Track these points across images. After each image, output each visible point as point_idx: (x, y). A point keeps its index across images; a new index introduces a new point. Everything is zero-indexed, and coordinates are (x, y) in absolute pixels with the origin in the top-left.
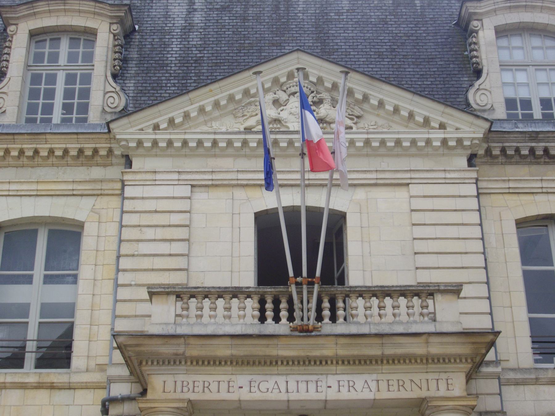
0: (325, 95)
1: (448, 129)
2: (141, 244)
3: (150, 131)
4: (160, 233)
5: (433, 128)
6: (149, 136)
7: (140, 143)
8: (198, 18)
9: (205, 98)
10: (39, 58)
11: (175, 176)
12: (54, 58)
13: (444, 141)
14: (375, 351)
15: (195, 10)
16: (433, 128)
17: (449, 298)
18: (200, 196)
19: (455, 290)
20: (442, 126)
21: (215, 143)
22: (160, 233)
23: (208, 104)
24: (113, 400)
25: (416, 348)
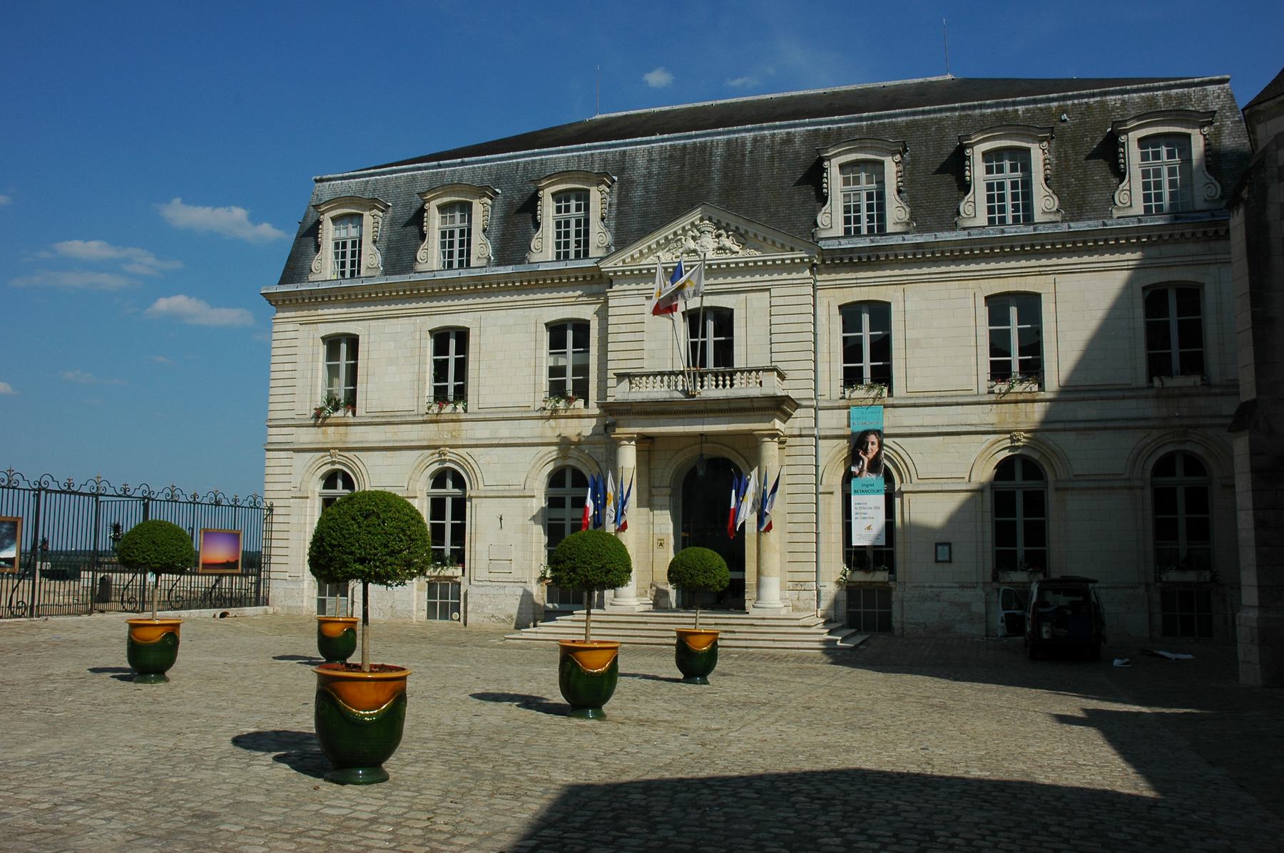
4: (629, 327)
8: (655, 169)
9: (651, 241)
10: (559, 210)
12: (567, 209)
22: (629, 327)
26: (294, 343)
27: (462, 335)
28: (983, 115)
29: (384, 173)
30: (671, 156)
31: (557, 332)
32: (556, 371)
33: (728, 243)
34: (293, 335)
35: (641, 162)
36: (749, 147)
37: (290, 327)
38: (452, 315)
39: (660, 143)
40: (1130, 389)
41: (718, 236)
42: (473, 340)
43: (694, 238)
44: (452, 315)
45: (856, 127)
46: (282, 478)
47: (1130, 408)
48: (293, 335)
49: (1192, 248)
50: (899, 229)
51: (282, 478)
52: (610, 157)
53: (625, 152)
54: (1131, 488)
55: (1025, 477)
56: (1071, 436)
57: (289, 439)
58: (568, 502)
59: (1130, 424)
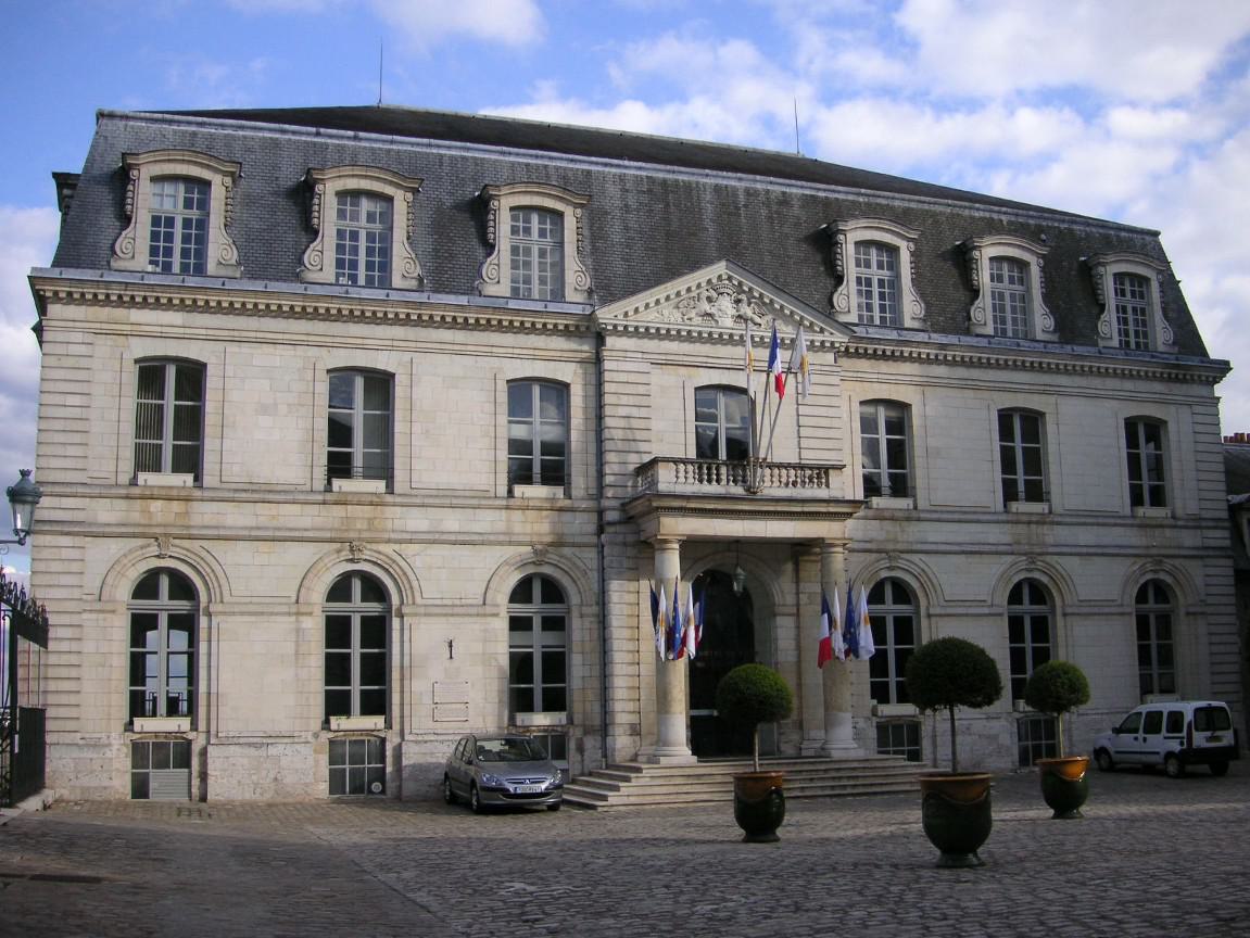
0: (743, 297)
1: (826, 333)
2: (620, 409)
3: (621, 317)
5: (816, 332)
6: (621, 322)
7: (615, 326)
9: (660, 292)
11: (640, 355)
13: (823, 342)
14: (799, 509)
15: (627, 191)
16: (816, 332)
17: (837, 472)
18: (656, 371)
19: (841, 468)
20: (822, 331)
21: (668, 330)
23: (662, 297)
24: (610, 524)
25: (822, 509)
26: (84, 363)
27: (381, 385)
28: (972, 218)
29: (189, 123)
30: (650, 191)
31: (519, 391)
32: (517, 446)
33: (747, 311)
34: (83, 350)
35: (613, 190)
36: (742, 198)
37: (78, 337)
38: (375, 348)
39: (633, 169)
40: (1120, 517)
41: (738, 301)
42: (400, 391)
43: (709, 299)
44: (375, 348)
45: (853, 202)
46: (65, 580)
47: (488, 521)
48: (83, 350)
49: (1158, 387)
50: (916, 325)
51: (65, 580)
52: (570, 174)
53: (589, 172)
54: (1122, 614)
55: (1032, 603)
56: (1076, 560)
57: (79, 516)
58: (537, 623)
59: (1122, 551)
